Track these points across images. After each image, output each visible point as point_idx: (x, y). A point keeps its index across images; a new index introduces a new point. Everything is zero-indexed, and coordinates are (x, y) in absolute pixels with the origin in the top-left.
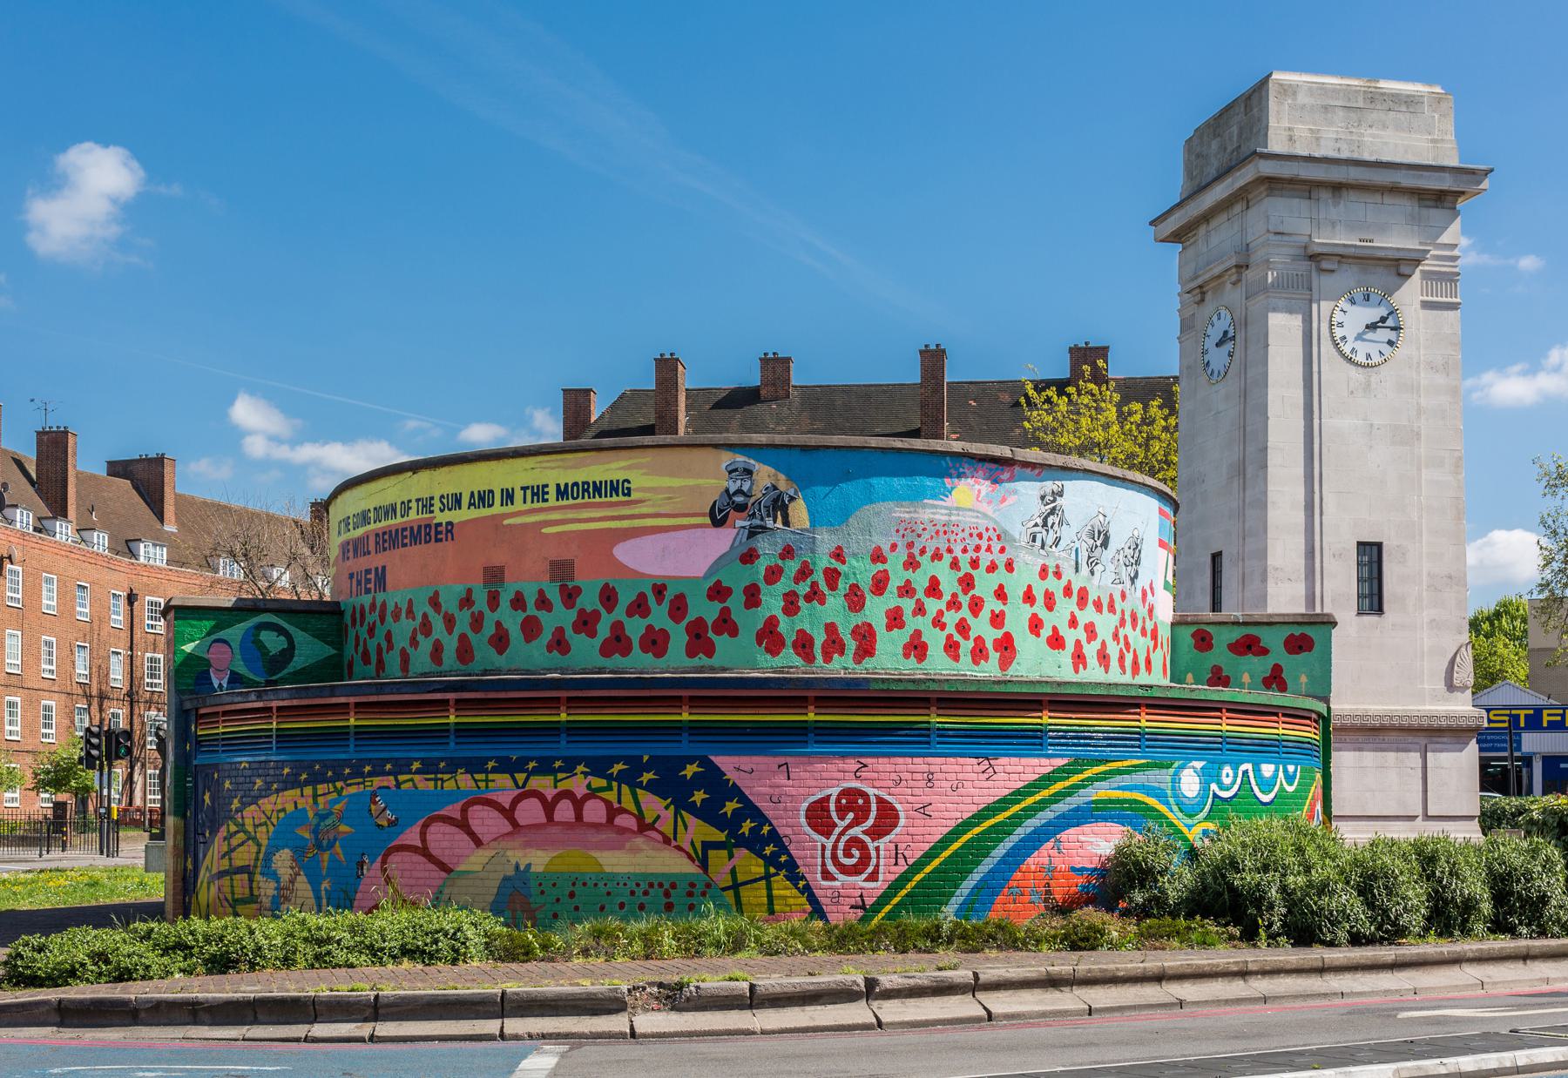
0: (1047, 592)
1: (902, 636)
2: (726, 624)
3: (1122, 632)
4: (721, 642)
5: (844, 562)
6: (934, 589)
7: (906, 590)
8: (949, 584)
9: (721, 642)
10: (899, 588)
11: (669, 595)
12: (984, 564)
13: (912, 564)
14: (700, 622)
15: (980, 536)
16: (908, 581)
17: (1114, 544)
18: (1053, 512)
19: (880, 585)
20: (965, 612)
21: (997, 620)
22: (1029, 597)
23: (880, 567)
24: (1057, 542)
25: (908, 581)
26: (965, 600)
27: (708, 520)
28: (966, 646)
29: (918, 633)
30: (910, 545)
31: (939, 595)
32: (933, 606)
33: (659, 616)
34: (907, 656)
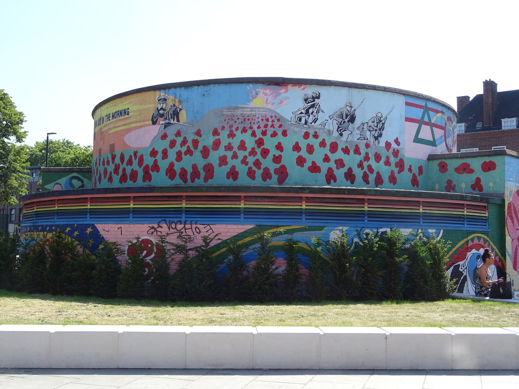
0: (308, 145)
1: (226, 169)
2: (156, 167)
3: (365, 164)
4: (154, 174)
5: (201, 136)
6: (242, 146)
7: (229, 147)
8: (250, 143)
9: (154, 174)
10: (225, 147)
11: (138, 155)
12: (269, 133)
13: (232, 135)
14: (147, 166)
15: (267, 120)
16: (230, 143)
17: (358, 122)
18: (313, 106)
19: (217, 145)
20: (259, 156)
21: (277, 159)
22: (297, 148)
23: (217, 137)
24: (315, 121)
25: (230, 143)
26: (259, 151)
27: (151, 122)
28: (259, 173)
29: (234, 167)
30: (231, 126)
31: (245, 149)
32: (241, 154)
33: (135, 166)
34: (228, 178)
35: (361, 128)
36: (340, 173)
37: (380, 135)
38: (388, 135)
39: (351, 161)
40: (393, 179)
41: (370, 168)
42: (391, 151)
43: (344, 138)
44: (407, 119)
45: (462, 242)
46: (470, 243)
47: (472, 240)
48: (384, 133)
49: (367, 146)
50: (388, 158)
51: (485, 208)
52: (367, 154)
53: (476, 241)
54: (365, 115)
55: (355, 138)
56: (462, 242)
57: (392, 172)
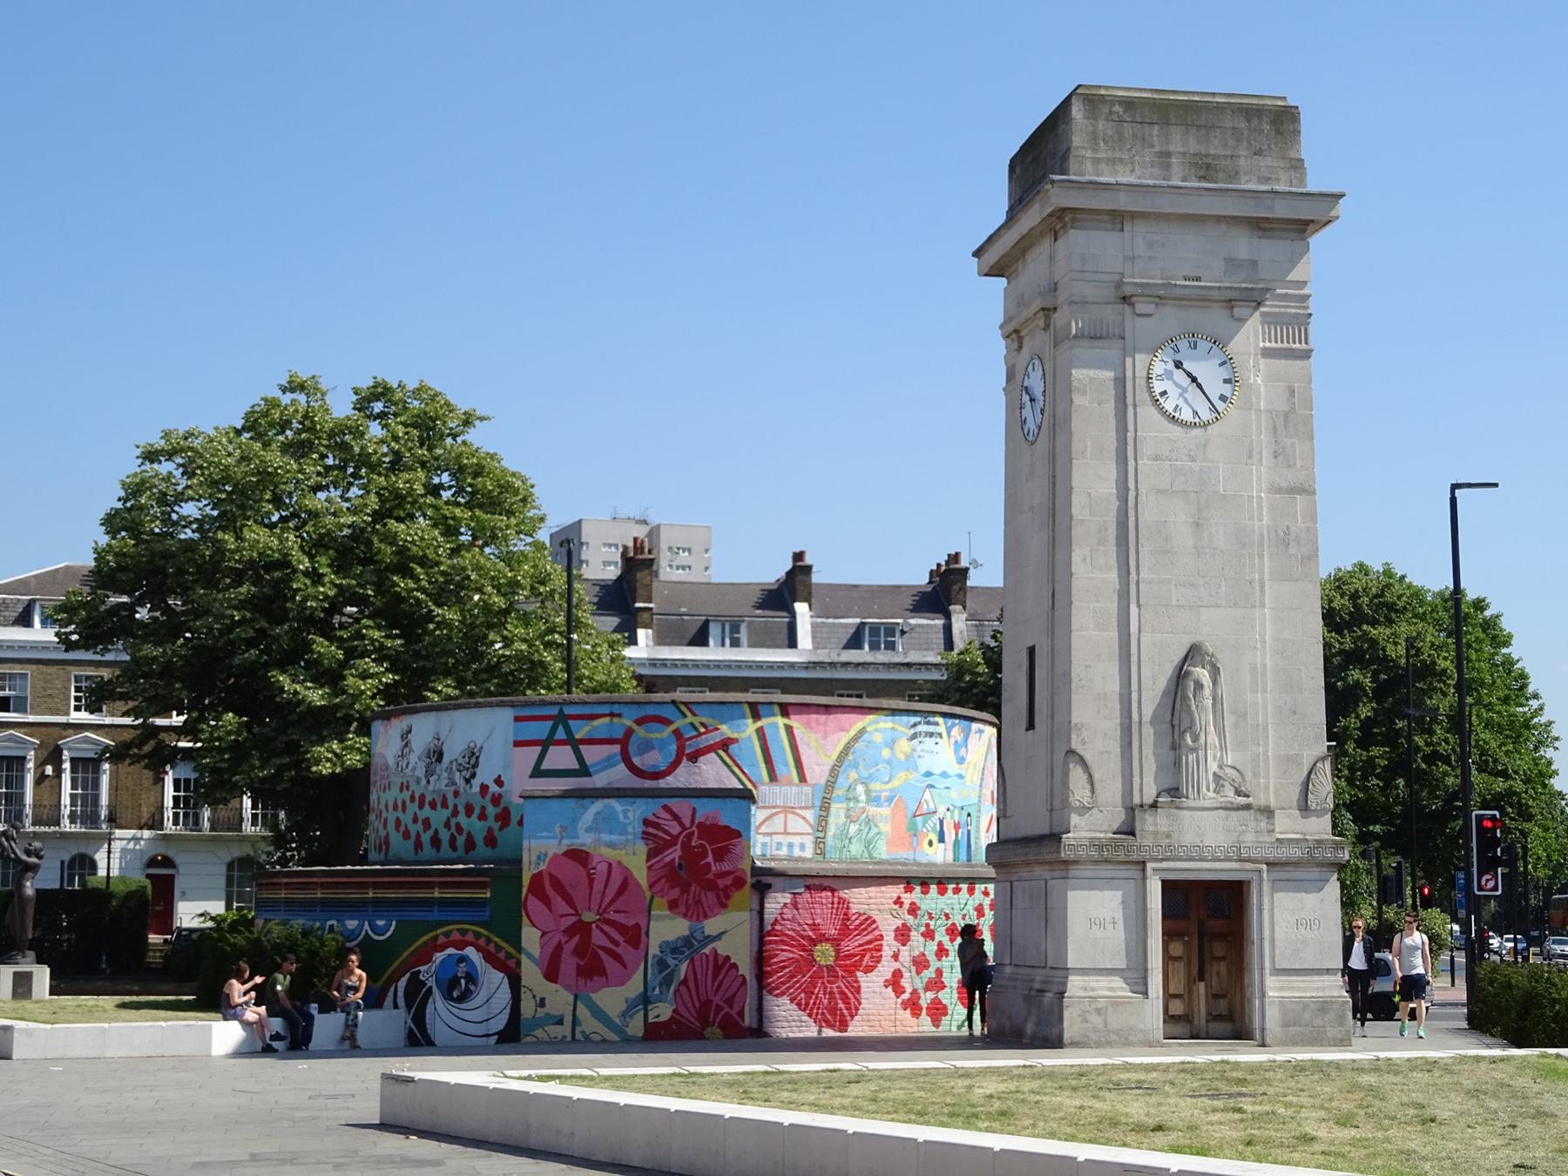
3: (453, 822)
17: (446, 760)
35: (449, 770)
36: (426, 838)
37: (473, 776)
38: (485, 775)
39: (438, 817)
40: (490, 840)
41: (459, 828)
42: (489, 797)
43: (431, 788)
44: (517, 744)
45: (425, 938)
46: (442, 940)
47: (447, 934)
48: (478, 771)
49: (456, 794)
50: (483, 808)
51: (483, 885)
52: (456, 806)
53: (456, 936)
54: (454, 751)
55: (442, 785)
56: (425, 938)
57: (490, 830)
